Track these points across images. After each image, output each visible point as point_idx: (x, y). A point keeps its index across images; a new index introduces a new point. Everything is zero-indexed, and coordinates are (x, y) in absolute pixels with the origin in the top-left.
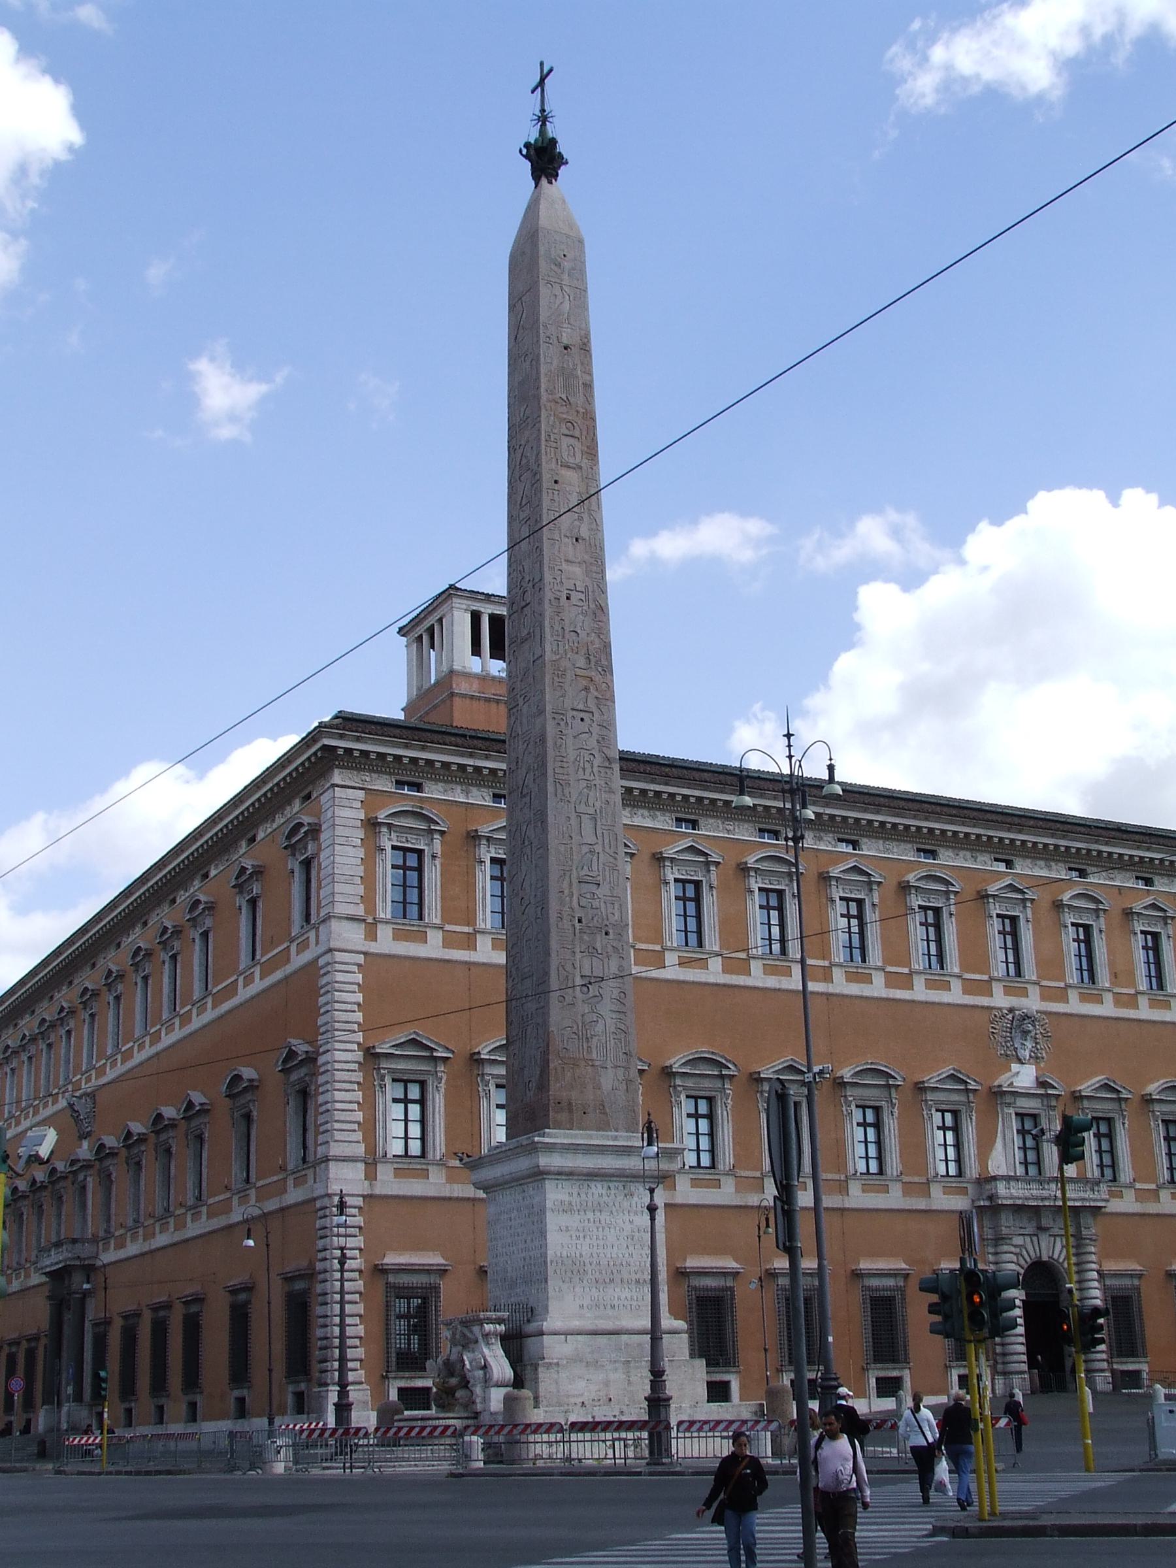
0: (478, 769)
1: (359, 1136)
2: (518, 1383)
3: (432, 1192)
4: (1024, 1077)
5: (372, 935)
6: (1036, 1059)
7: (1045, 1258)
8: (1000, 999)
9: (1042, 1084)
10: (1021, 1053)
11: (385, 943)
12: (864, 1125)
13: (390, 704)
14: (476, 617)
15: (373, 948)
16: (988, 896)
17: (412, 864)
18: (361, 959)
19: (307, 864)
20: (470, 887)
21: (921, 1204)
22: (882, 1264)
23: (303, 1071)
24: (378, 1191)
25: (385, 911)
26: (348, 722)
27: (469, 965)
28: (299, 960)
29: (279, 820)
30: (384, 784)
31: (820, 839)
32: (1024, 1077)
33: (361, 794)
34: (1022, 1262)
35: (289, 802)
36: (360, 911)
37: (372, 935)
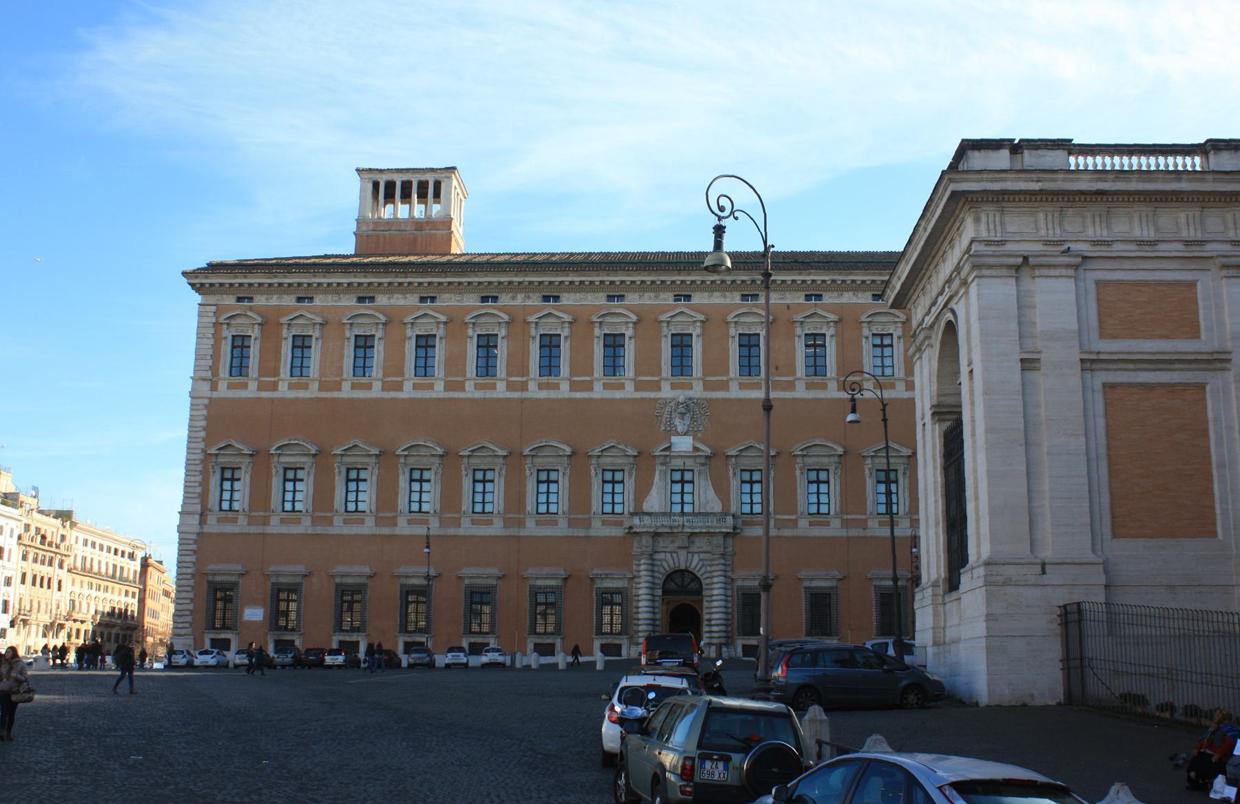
0: (280, 284)
1: (197, 501)
3: (237, 530)
4: (683, 444)
5: (214, 387)
7: (683, 567)
8: (666, 392)
9: (696, 449)
10: (680, 429)
11: (223, 391)
15: (215, 395)
16: (661, 322)
17: (240, 344)
18: (206, 401)
21: (582, 533)
22: (546, 571)
24: (206, 529)
25: (224, 371)
27: (272, 400)
31: (529, 298)
32: (683, 444)
33: (214, 308)
34: (662, 570)
36: (209, 375)
37: (214, 387)
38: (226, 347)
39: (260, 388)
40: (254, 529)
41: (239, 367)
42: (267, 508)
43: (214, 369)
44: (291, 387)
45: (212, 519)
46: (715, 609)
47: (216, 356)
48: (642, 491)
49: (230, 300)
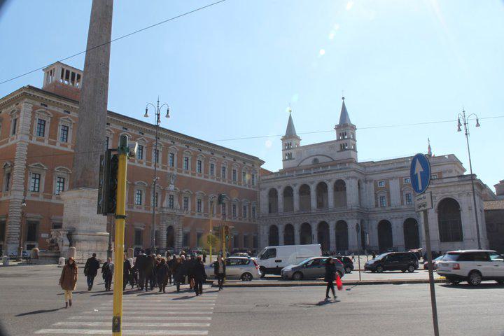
0: (61, 104)
2: (71, 245)
5: (31, 139)
6: (174, 184)
8: (169, 171)
9: (175, 189)
11: (34, 141)
12: (138, 194)
13: (40, 86)
14: (63, 70)
15: (32, 142)
17: (42, 123)
19: (16, 120)
20: (56, 131)
23: (9, 169)
25: (35, 133)
26: (30, 88)
28: (11, 143)
29: (9, 109)
30: (38, 104)
35: (12, 105)
37: (31, 139)
38: (36, 122)
39: (49, 143)
40: (46, 200)
41: (41, 132)
42: (51, 192)
43: (31, 131)
44: (61, 145)
45: (29, 194)
46: (179, 240)
47: (32, 126)
48: (163, 200)
49: (38, 104)
